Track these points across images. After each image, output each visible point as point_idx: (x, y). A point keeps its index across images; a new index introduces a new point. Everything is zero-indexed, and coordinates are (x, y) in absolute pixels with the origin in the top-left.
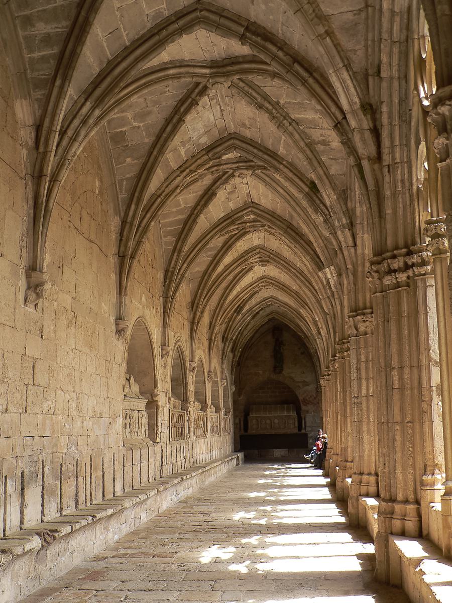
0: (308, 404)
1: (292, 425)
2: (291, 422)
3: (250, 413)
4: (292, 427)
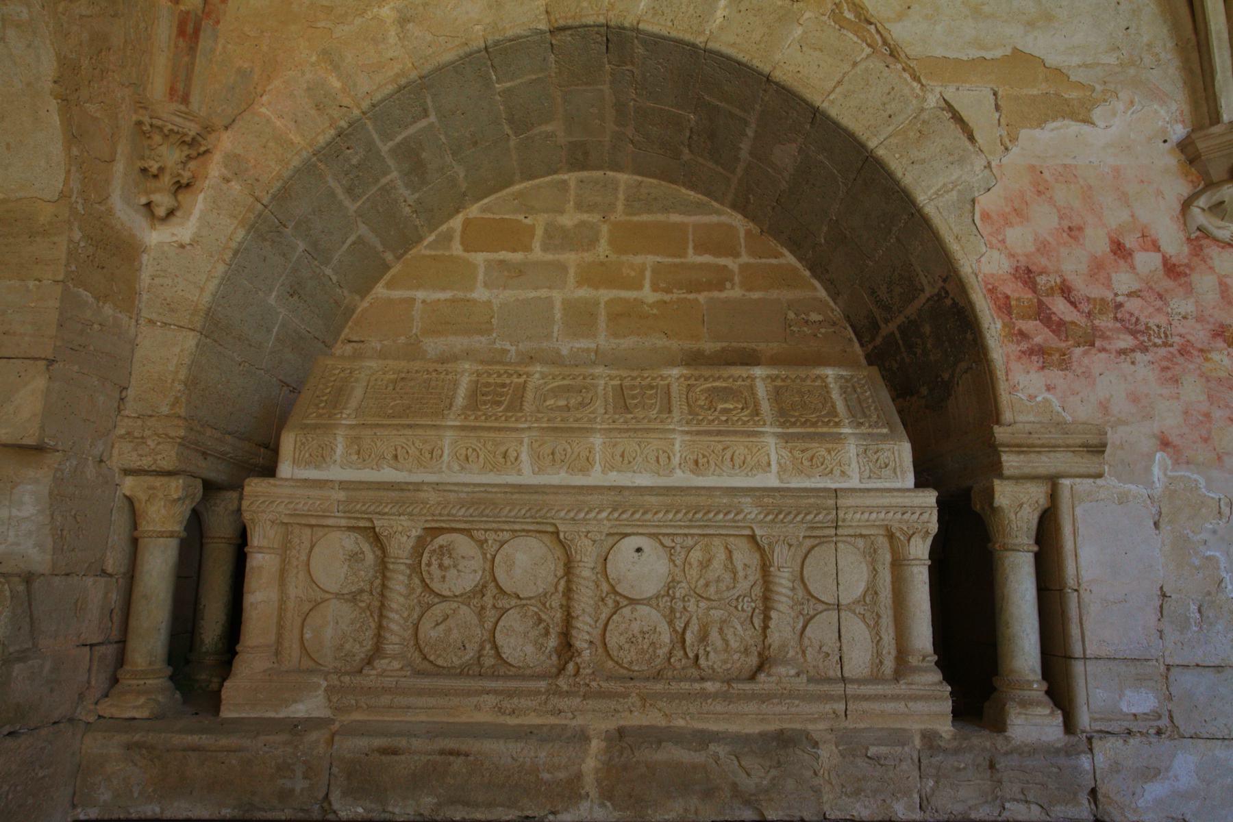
0: (1089, 340)
1: (857, 630)
2: (855, 581)
3: (288, 442)
4: (859, 660)
